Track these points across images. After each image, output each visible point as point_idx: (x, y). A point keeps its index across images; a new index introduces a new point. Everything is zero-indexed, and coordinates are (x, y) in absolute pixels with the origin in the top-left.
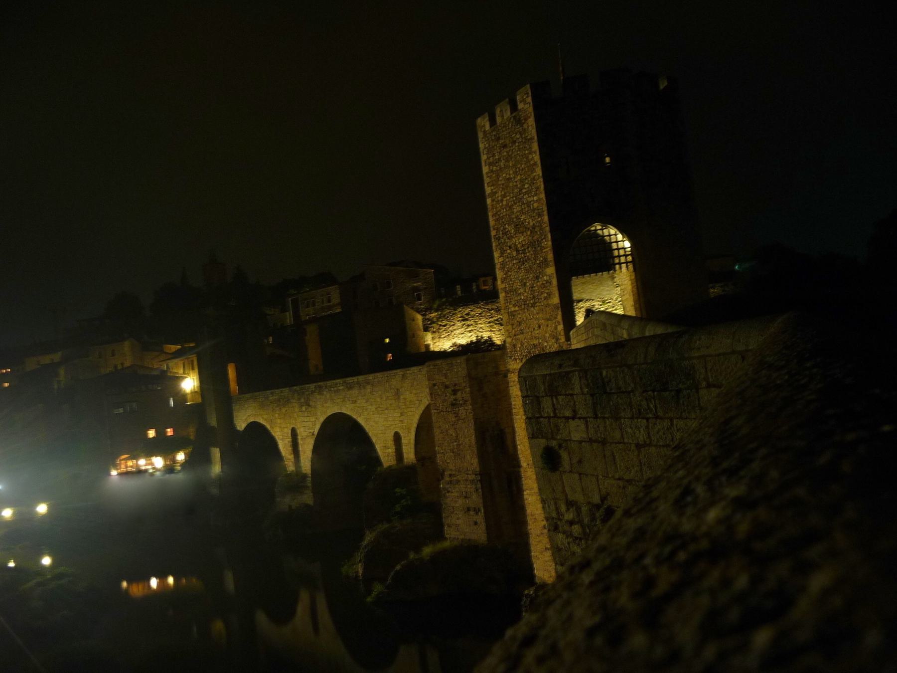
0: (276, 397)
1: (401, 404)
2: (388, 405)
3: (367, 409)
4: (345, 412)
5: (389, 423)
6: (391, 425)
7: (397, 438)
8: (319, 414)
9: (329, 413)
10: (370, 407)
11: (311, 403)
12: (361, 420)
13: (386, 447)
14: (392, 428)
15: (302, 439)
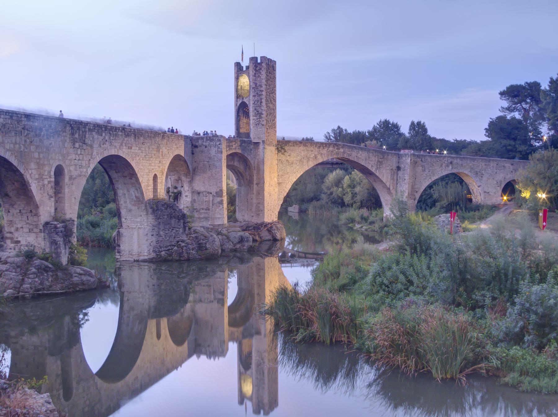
0: (36, 124)
1: (160, 155)
2: (153, 155)
3: (139, 156)
4: (121, 155)
5: (152, 167)
6: (153, 169)
7: (155, 177)
8: (95, 153)
9: (106, 154)
10: (141, 154)
11: (88, 141)
12: (133, 164)
13: (148, 186)
14: (153, 171)
15: (71, 178)
